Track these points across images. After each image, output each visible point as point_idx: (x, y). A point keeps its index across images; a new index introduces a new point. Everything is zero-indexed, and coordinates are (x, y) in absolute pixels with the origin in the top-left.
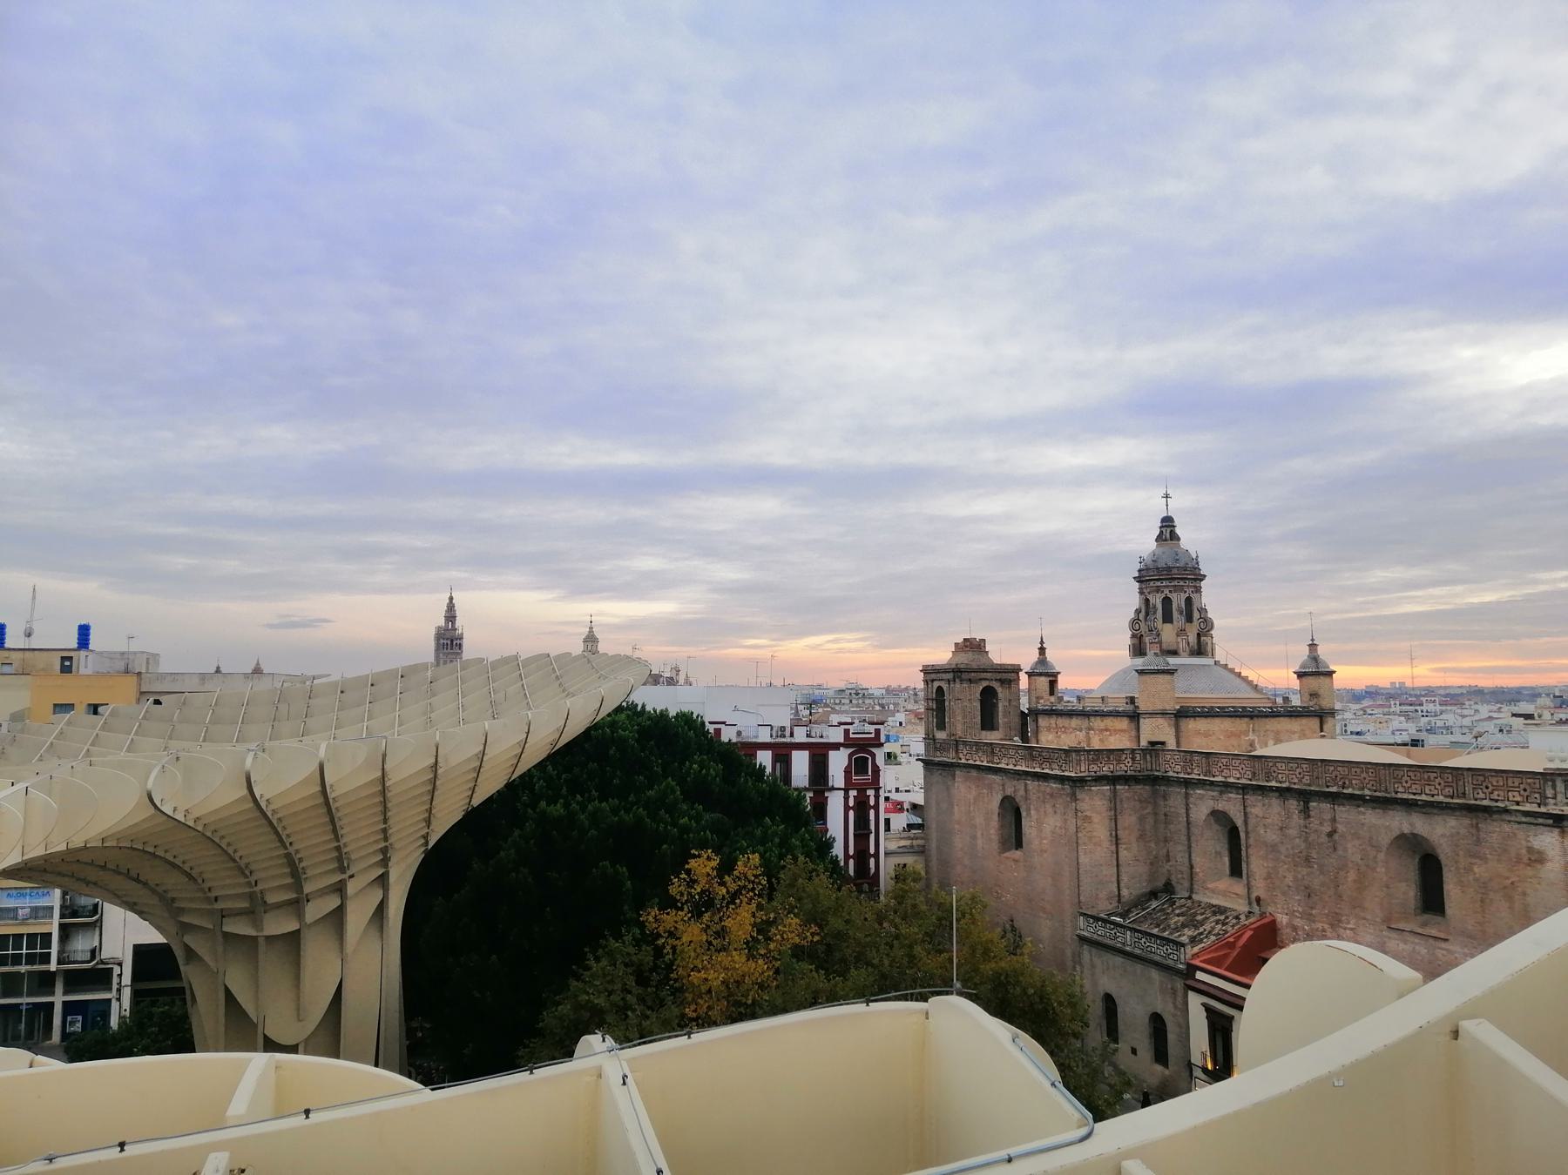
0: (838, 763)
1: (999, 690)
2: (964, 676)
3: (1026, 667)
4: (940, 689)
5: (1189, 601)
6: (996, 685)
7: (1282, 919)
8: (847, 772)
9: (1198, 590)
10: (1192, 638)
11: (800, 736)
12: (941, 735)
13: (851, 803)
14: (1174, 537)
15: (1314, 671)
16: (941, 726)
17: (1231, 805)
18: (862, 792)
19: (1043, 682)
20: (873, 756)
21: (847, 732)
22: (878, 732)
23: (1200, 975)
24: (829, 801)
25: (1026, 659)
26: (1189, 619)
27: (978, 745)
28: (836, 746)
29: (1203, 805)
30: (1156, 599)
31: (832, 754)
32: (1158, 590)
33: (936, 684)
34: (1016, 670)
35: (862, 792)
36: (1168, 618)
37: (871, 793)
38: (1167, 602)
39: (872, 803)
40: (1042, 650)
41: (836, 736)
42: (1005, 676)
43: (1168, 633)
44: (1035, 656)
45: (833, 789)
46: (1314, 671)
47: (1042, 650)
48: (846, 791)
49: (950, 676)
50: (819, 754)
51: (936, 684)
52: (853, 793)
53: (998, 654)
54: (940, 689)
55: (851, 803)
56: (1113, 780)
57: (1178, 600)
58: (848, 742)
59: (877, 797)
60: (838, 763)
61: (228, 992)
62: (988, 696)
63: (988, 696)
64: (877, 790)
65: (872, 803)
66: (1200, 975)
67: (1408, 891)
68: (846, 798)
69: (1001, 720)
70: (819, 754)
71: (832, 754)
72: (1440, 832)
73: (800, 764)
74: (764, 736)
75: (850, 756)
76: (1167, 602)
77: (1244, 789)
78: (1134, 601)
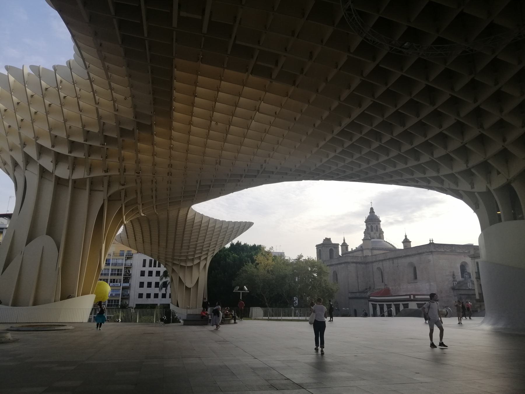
3: (341, 244)
5: (377, 226)
7: (390, 288)
9: (380, 224)
10: (378, 235)
14: (373, 212)
15: (406, 241)
17: (380, 265)
19: (344, 247)
23: (371, 298)
25: (341, 243)
26: (377, 230)
29: (376, 266)
30: (370, 226)
32: (370, 224)
34: (338, 244)
36: (372, 231)
38: (372, 227)
40: (344, 240)
43: (372, 233)
44: (343, 242)
46: (406, 241)
47: (344, 240)
53: (333, 241)
56: (356, 263)
57: (374, 226)
61: (179, 277)
62: (331, 251)
63: (331, 251)
66: (371, 298)
67: (412, 275)
72: (415, 260)
76: (372, 227)
77: (382, 261)
78: (365, 227)
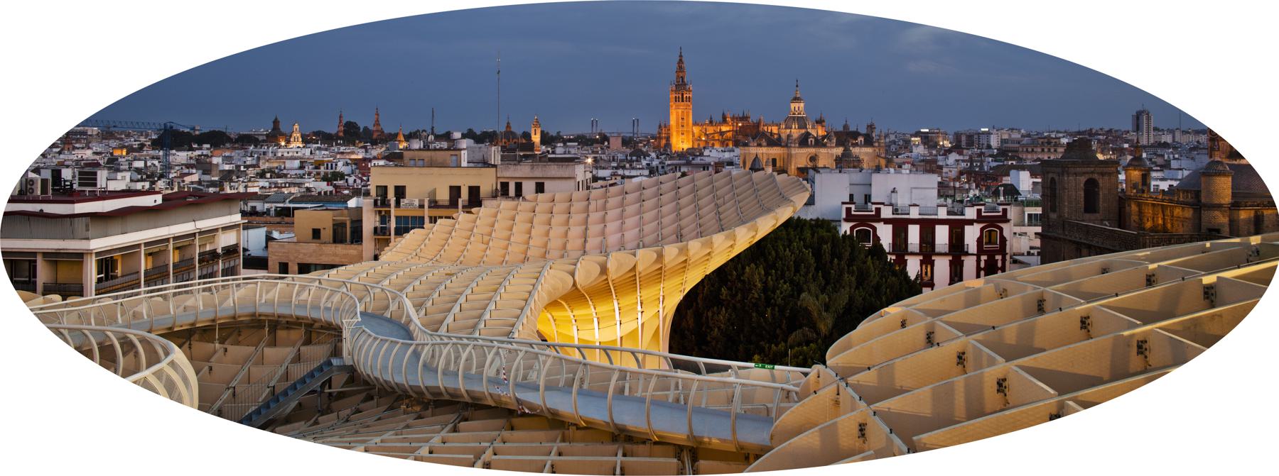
0: (972, 234)
1: (1102, 182)
2: (1072, 170)
4: (1053, 179)
6: (1096, 176)
8: (980, 241)
11: (942, 214)
12: (1053, 216)
13: (982, 265)
16: (1053, 210)
18: (991, 255)
20: (1001, 229)
21: (979, 211)
22: (1005, 211)
24: (965, 263)
27: (1080, 228)
28: (971, 222)
31: (968, 228)
33: (1050, 176)
35: (991, 255)
37: (999, 257)
39: (1000, 264)
41: (970, 213)
42: (1105, 170)
45: (967, 254)
48: (978, 256)
49: (1059, 170)
50: (956, 229)
51: (1050, 176)
52: (984, 258)
54: (1053, 179)
55: (982, 265)
58: (980, 218)
59: (1004, 260)
60: (972, 234)
63: (1091, 186)
64: (1003, 253)
65: (1000, 264)
68: (978, 261)
69: (1102, 204)
70: (956, 229)
71: (968, 228)
73: (942, 235)
74: (914, 214)
75: (982, 230)
